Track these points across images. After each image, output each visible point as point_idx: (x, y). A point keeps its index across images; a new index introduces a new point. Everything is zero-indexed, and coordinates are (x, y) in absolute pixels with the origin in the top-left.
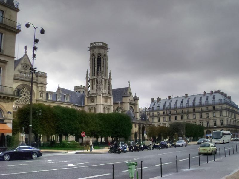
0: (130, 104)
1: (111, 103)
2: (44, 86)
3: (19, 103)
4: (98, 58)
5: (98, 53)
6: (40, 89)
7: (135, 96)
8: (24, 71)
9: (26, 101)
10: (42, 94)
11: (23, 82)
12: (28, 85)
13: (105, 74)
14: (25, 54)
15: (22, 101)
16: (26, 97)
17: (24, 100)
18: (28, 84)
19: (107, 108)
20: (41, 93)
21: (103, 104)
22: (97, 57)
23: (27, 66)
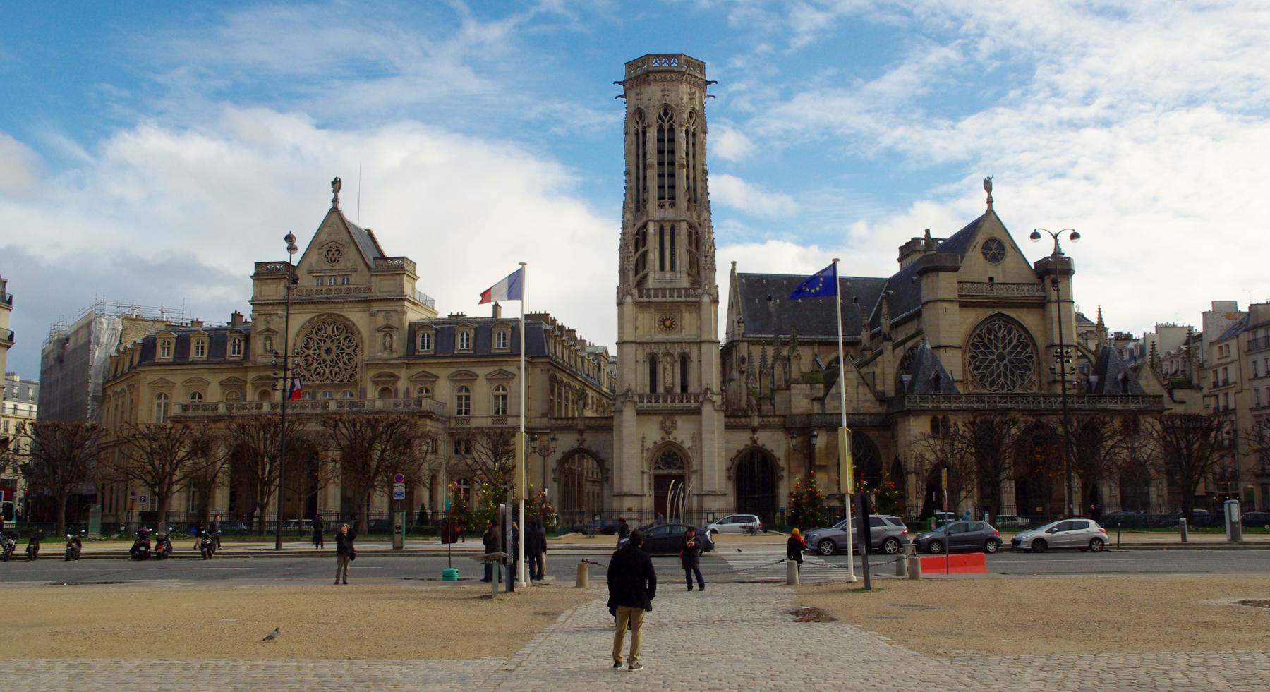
0: (965, 303)
1: (700, 328)
2: (394, 308)
3: (309, 383)
4: (637, 135)
5: (634, 109)
6: (381, 321)
7: (1057, 252)
8: (330, 268)
9: (336, 369)
10: (391, 336)
11: (320, 306)
12: (339, 316)
13: (672, 198)
14: (331, 205)
15: (319, 373)
16: (321, 360)
17: (328, 371)
18: (337, 311)
19: (668, 354)
20: (385, 336)
21: (647, 338)
22: (632, 131)
23: (341, 248)
